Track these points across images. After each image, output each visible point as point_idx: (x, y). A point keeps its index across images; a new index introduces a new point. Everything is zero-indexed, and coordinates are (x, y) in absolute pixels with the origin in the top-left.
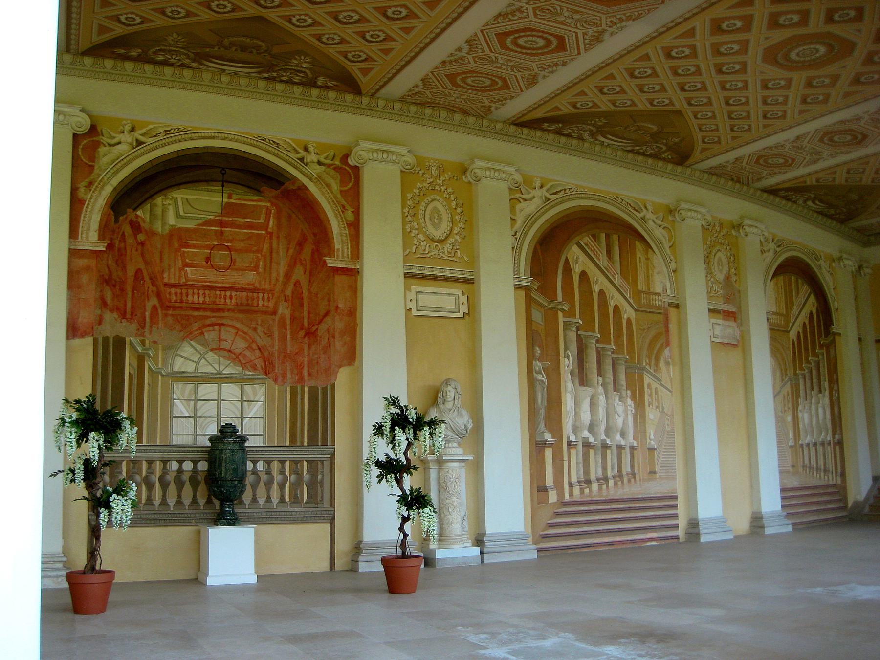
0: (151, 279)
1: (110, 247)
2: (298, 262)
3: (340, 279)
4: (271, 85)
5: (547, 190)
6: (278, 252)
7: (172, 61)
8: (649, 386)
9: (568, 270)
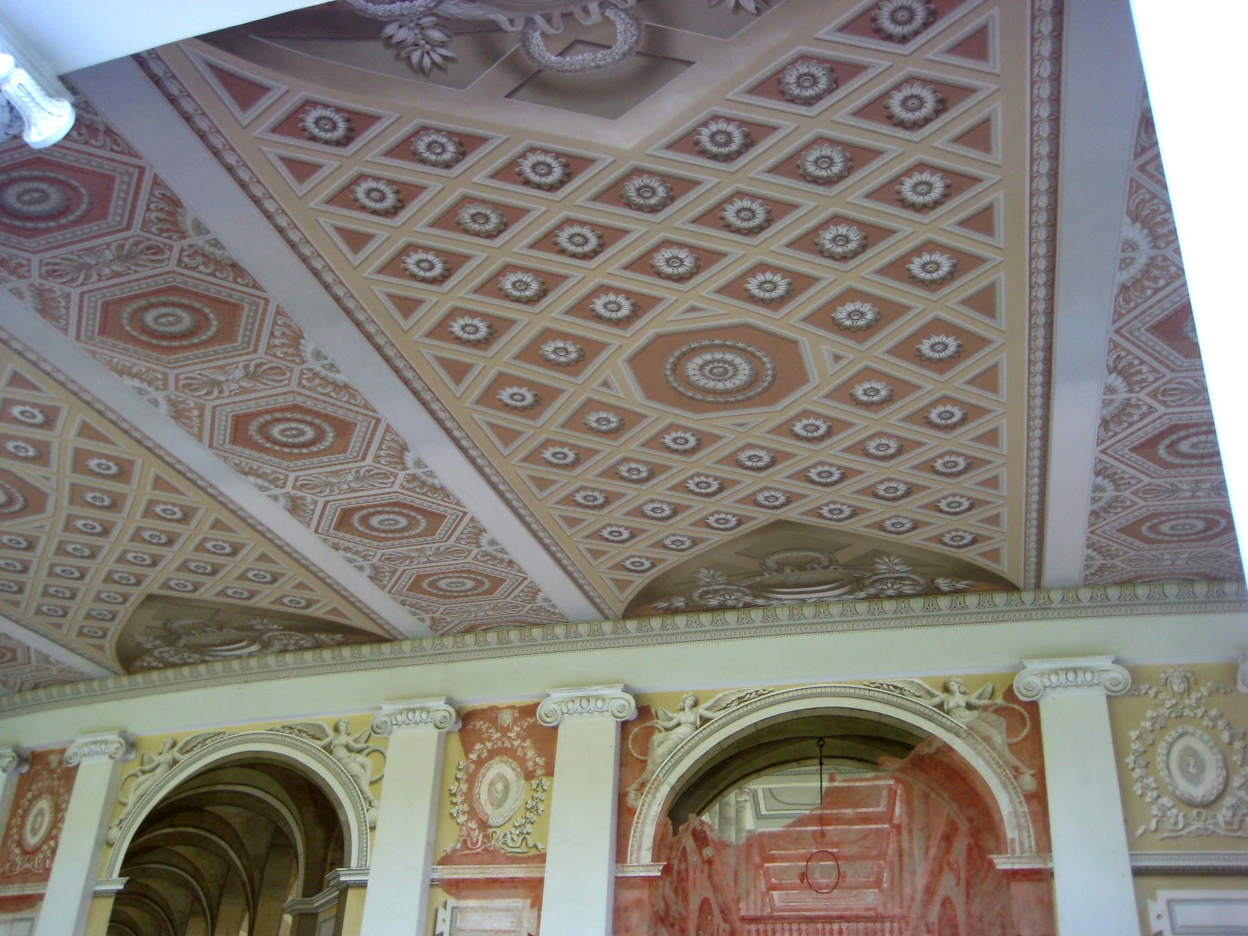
0: (722, 912)
1: (667, 870)
2: (946, 867)
3: (1020, 890)
4: (875, 605)
6: (911, 855)
7: (730, 603)
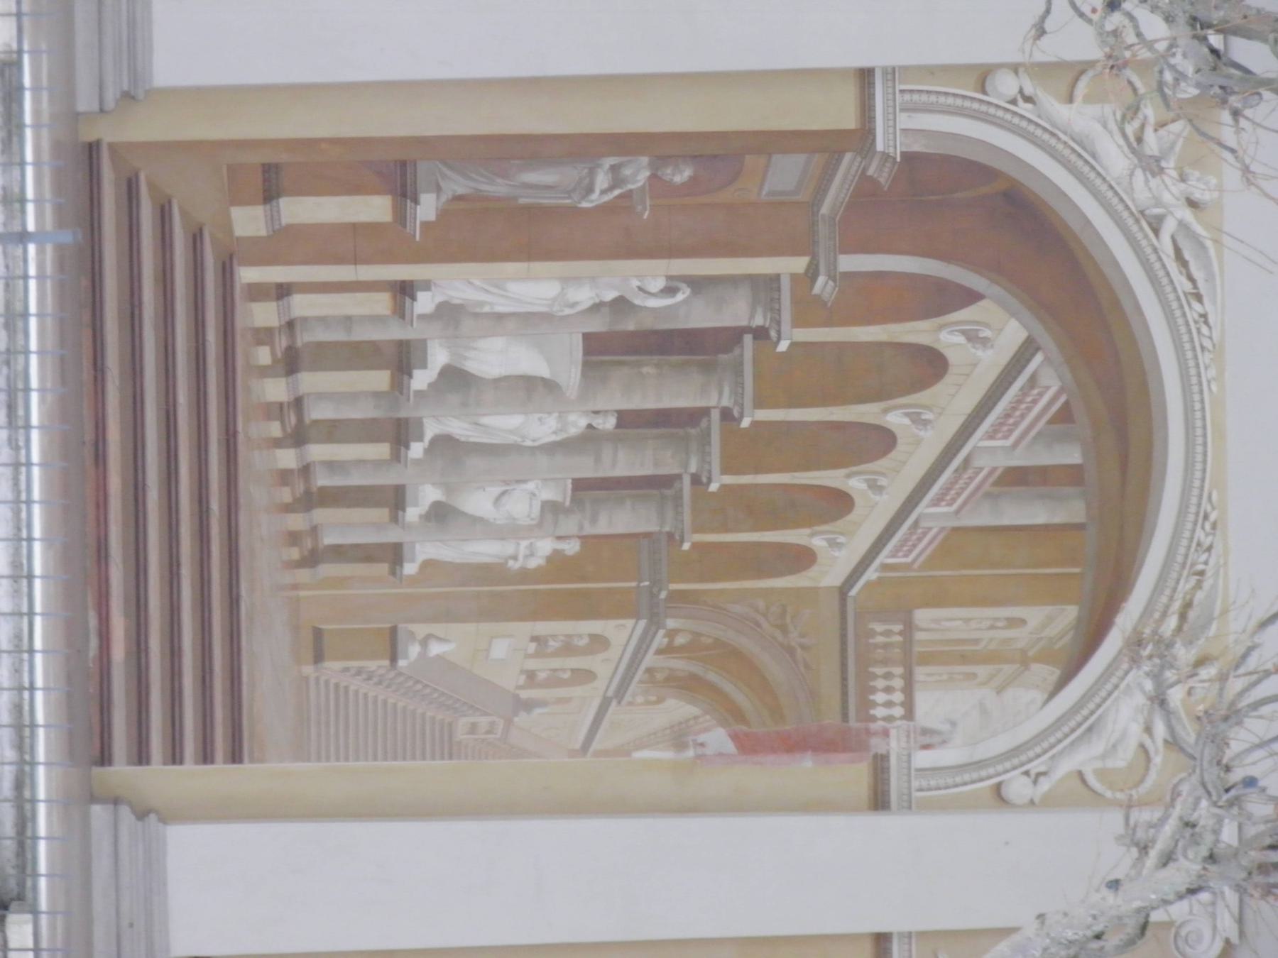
5: (1182, 225)
8: (599, 643)
9: (943, 299)
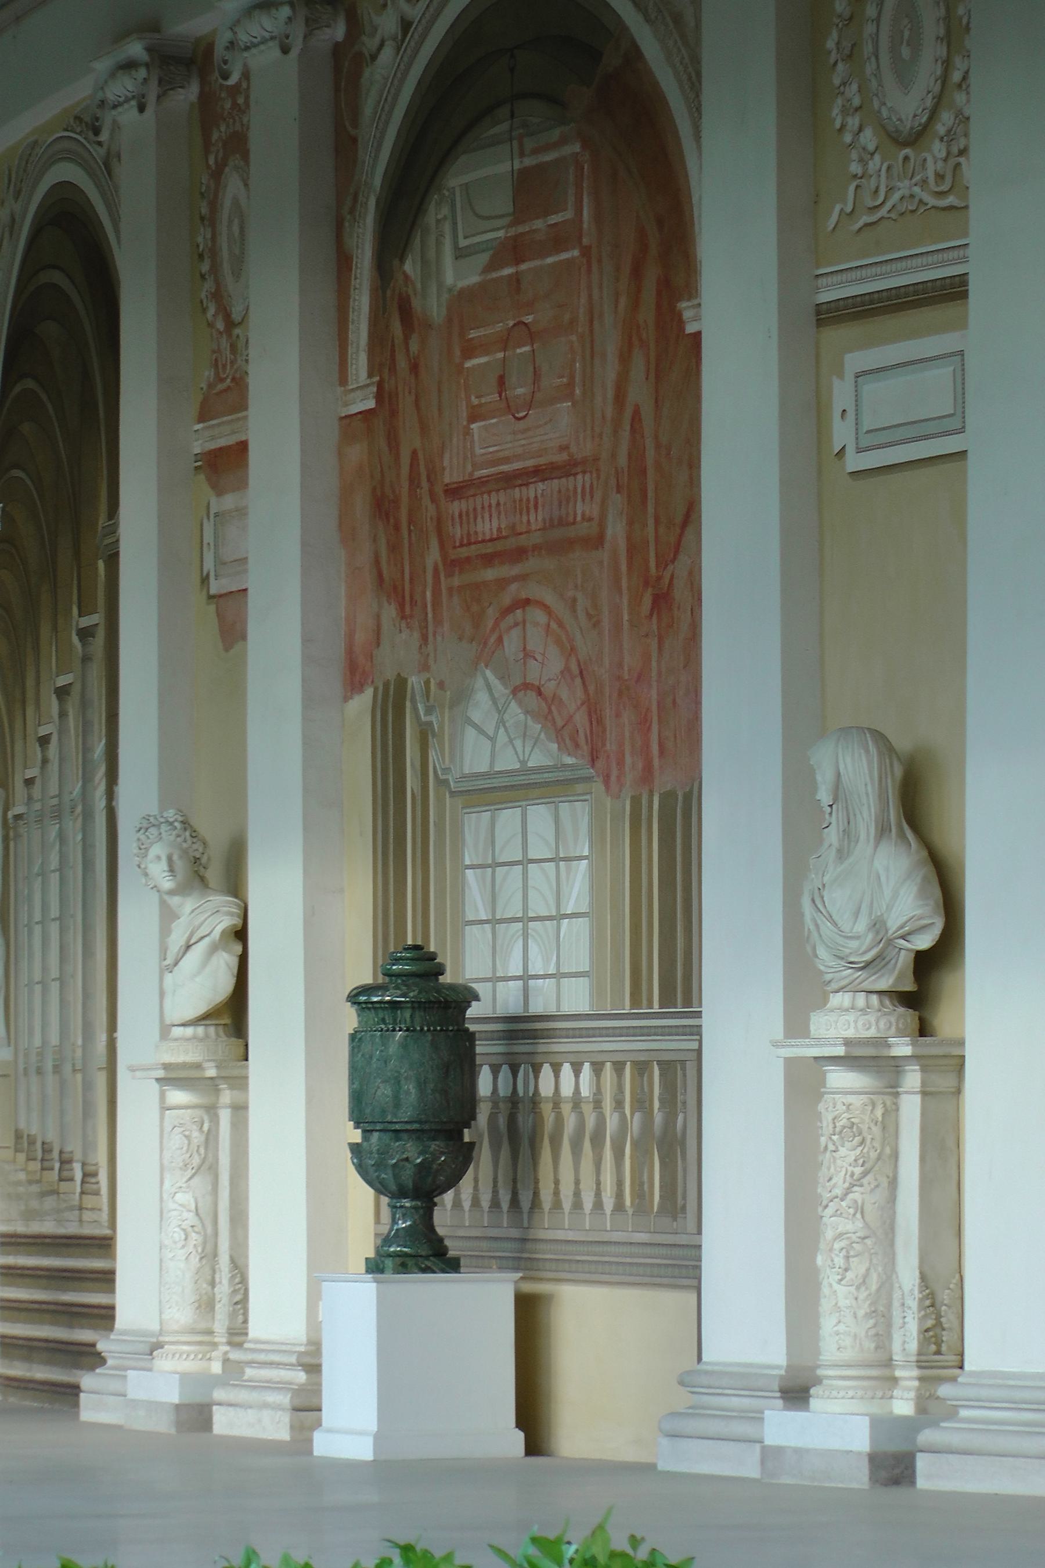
1: (379, 397)
